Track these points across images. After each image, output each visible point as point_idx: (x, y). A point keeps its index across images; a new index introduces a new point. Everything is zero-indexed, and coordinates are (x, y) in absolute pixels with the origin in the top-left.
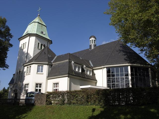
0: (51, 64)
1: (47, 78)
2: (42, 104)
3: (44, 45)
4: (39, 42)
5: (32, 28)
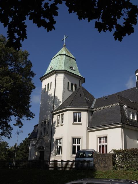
0: (92, 110)
1: (88, 130)
2: (107, 168)
3: (76, 84)
4: (69, 81)
5: (58, 62)
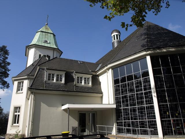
4: (41, 54)
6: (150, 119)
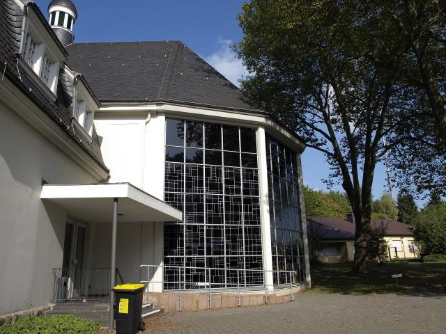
6: (251, 254)
